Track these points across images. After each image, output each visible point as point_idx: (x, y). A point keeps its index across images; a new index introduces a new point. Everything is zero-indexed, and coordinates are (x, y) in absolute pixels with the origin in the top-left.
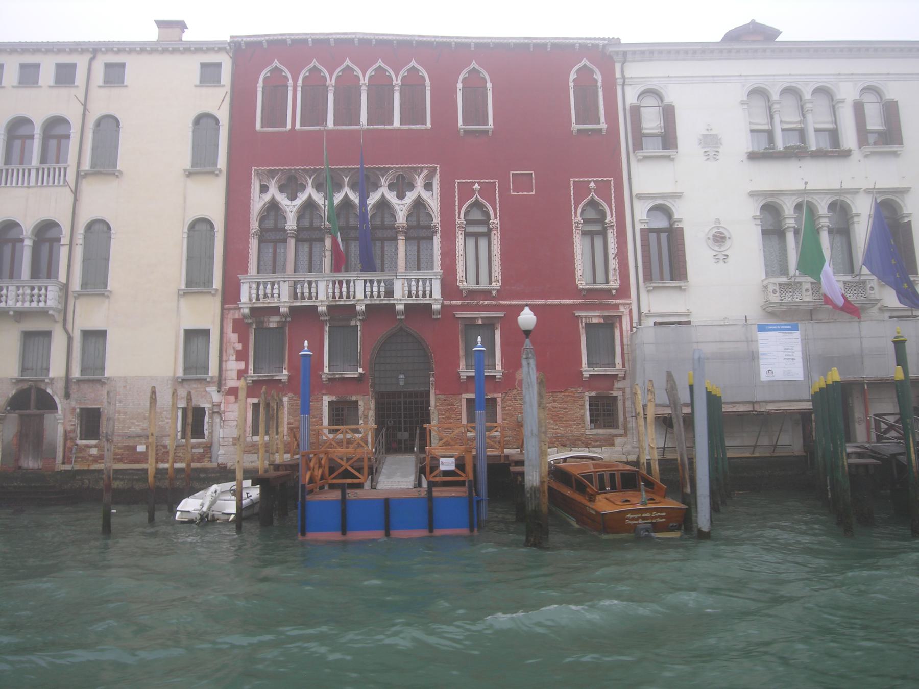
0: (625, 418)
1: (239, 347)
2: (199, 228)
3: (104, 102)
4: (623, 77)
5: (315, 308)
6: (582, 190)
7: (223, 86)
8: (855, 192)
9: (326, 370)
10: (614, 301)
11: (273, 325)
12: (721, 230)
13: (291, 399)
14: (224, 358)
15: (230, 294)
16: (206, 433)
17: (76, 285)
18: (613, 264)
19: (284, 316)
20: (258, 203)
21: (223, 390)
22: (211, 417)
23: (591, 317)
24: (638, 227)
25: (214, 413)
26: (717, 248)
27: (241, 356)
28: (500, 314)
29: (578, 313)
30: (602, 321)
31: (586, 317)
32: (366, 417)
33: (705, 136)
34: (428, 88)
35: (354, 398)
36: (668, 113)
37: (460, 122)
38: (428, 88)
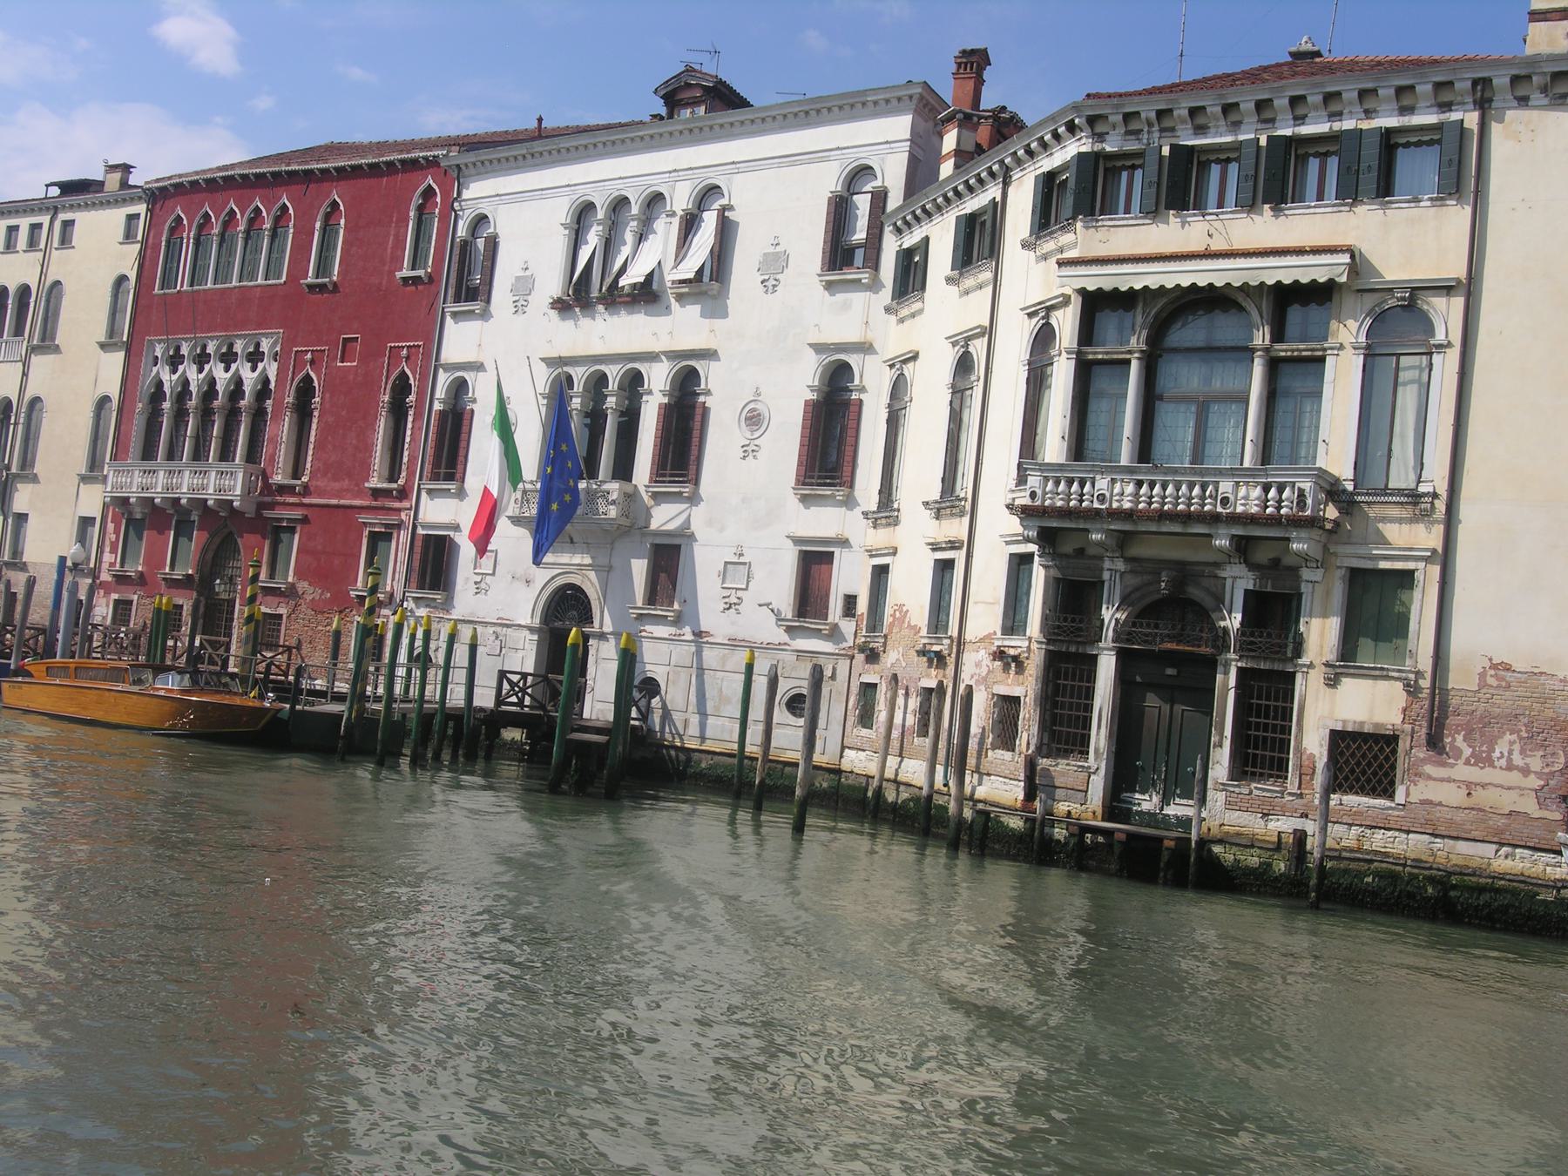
1: (113, 537)
3: (62, 265)
8: (652, 357)
10: (397, 505)
17: (14, 470)
24: (437, 406)
27: (114, 550)
28: (297, 514)
29: (363, 518)
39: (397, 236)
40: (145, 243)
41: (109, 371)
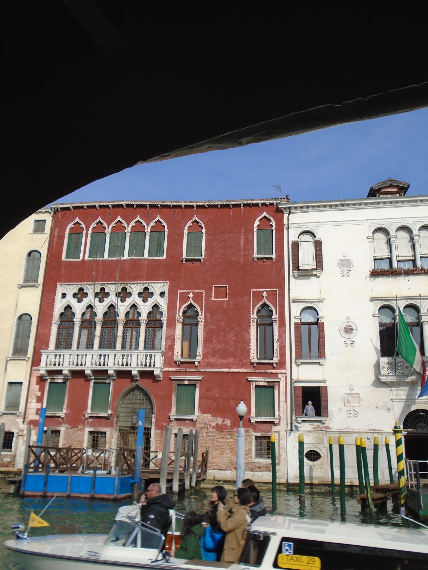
0: (279, 452)
1: (39, 394)
2: (23, 319)
4: (288, 224)
5: (83, 371)
6: (258, 296)
7: (46, 234)
9: (89, 411)
11: (61, 381)
12: (350, 324)
13: (67, 428)
14: (29, 400)
15: (36, 361)
16: (13, 448)
18: (276, 346)
19: (66, 375)
20: (59, 306)
21: (26, 421)
22: (17, 438)
23: (259, 381)
25: (20, 435)
26: (346, 336)
27: (40, 400)
30: (266, 384)
31: (255, 381)
32: (110, 443)
33: (342, 261)
34: (166, 234)
35: (104, 430)
36: (318, 246)
37: (184, 253)
38: (166, 234)
39: (246, 239)
40: (52, 233)
41: (30, 301)
